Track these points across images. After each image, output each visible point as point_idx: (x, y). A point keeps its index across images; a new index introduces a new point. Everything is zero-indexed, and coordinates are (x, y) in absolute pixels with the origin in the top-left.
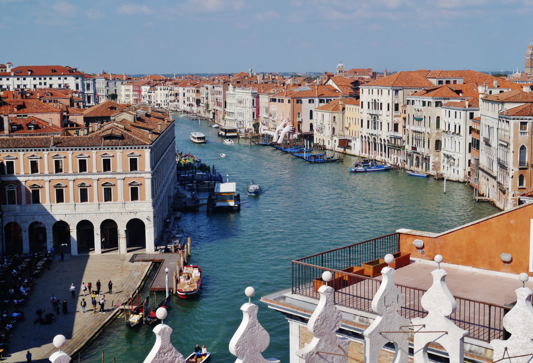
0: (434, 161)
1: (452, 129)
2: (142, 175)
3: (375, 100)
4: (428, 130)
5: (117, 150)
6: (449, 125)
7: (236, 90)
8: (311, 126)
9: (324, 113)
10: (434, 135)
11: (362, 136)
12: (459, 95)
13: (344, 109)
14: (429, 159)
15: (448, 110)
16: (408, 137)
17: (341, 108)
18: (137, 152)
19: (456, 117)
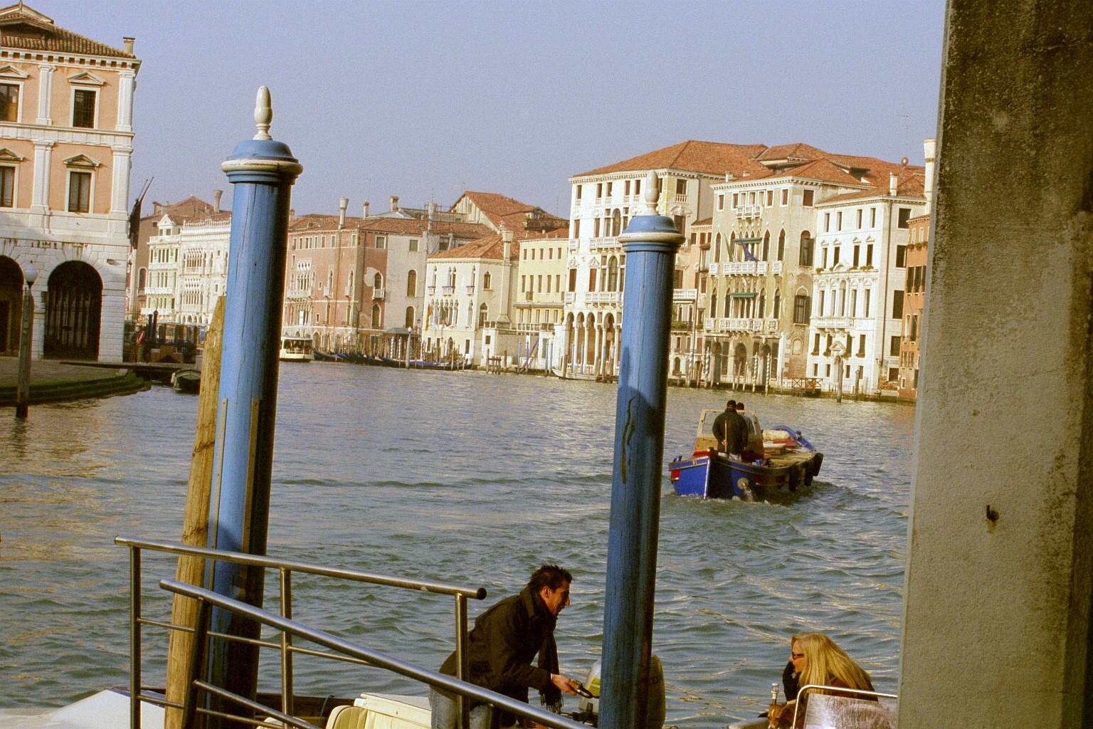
0: (789, 351)
1: (847, 257)
2: (108, 140)
3: (617, 211)
4: (777, 266)
5: (40, 63)
6: (837, 250)
7: (183, 232)
8: (410, 311)
9: (458, 266)
10: (792, 282)
11: (571, 316)
12: (860, 180)
13: (514, 258)
14: (776, 346)
15: (834, 213)
16: (714, 297)
17: (506, 252)
18: (97, 76)
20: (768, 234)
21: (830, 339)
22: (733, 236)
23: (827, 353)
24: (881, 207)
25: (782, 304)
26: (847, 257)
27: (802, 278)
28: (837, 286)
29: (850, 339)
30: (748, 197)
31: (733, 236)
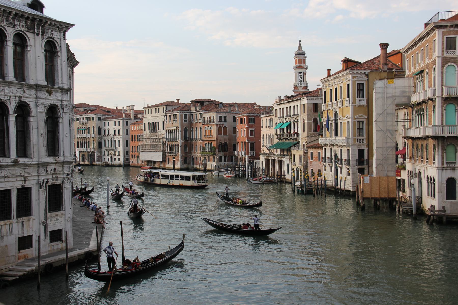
4: (93, 135)
6: (109, 131)
10: (97, 139)
14: (94, 154)
19: (115, 125)
20: (89, 128)
21: (108, 152)
22: (78, 128)
23: (108, 155)
24: (121, 122)
25: (95, 145)
26: (112, 132)
27: (99, 138)
28: (110, 140)
29: (115, 152)
30: (82, 119)
31: (78, 128)
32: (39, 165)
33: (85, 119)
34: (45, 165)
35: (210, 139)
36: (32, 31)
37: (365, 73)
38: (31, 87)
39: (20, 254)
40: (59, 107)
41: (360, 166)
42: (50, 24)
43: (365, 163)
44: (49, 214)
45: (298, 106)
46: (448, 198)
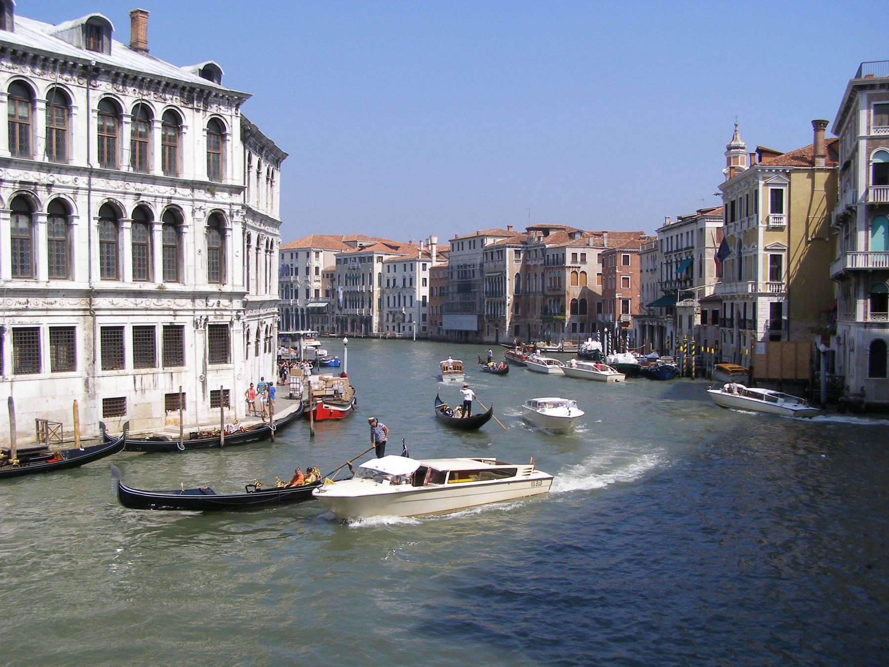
6: (394, 280)
21: (394, 316)
23: (393, 321)
32: (194, 296)
33: (357, 260)
34: (206, 296)
35: (557, 293)
36: (190, 106)
37: (784, 171)
38: (186, 184)
39: (168, 418)
40: (227, 212)
41: (773, 331)
42: (216, 96)
43: (783, 326)
44: (209, 367)
45: (692, 231)
46: (872, 374)
